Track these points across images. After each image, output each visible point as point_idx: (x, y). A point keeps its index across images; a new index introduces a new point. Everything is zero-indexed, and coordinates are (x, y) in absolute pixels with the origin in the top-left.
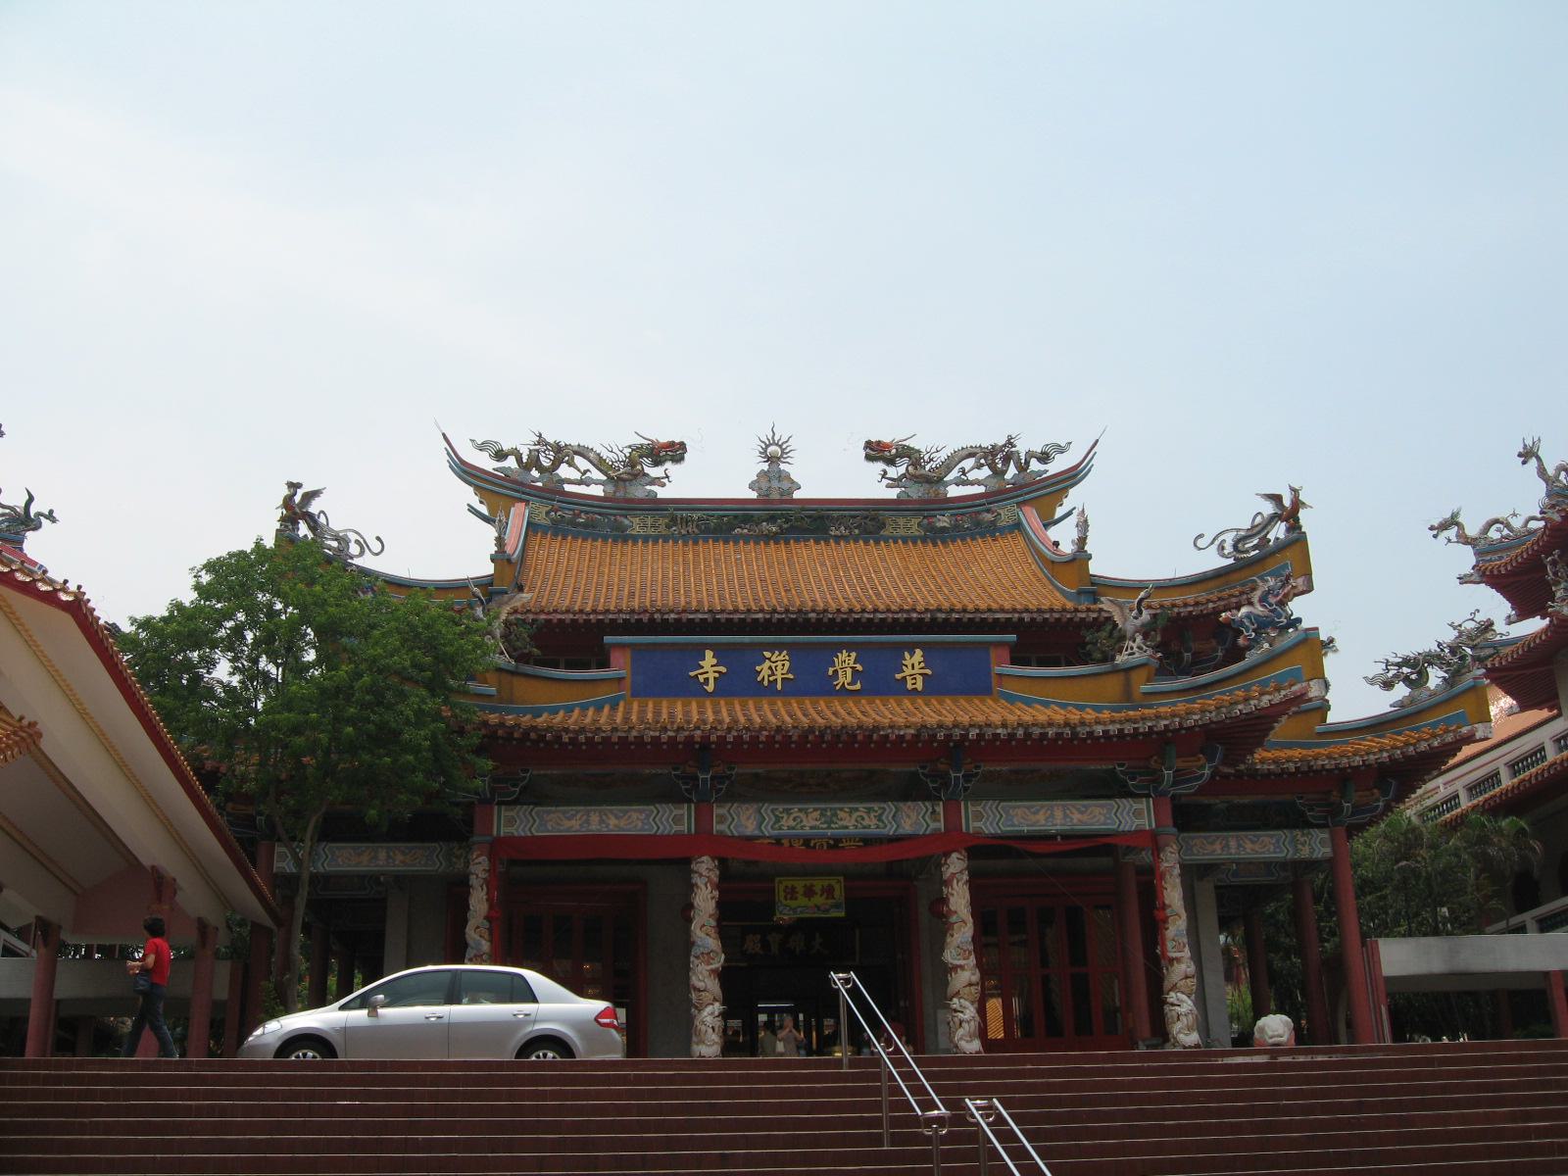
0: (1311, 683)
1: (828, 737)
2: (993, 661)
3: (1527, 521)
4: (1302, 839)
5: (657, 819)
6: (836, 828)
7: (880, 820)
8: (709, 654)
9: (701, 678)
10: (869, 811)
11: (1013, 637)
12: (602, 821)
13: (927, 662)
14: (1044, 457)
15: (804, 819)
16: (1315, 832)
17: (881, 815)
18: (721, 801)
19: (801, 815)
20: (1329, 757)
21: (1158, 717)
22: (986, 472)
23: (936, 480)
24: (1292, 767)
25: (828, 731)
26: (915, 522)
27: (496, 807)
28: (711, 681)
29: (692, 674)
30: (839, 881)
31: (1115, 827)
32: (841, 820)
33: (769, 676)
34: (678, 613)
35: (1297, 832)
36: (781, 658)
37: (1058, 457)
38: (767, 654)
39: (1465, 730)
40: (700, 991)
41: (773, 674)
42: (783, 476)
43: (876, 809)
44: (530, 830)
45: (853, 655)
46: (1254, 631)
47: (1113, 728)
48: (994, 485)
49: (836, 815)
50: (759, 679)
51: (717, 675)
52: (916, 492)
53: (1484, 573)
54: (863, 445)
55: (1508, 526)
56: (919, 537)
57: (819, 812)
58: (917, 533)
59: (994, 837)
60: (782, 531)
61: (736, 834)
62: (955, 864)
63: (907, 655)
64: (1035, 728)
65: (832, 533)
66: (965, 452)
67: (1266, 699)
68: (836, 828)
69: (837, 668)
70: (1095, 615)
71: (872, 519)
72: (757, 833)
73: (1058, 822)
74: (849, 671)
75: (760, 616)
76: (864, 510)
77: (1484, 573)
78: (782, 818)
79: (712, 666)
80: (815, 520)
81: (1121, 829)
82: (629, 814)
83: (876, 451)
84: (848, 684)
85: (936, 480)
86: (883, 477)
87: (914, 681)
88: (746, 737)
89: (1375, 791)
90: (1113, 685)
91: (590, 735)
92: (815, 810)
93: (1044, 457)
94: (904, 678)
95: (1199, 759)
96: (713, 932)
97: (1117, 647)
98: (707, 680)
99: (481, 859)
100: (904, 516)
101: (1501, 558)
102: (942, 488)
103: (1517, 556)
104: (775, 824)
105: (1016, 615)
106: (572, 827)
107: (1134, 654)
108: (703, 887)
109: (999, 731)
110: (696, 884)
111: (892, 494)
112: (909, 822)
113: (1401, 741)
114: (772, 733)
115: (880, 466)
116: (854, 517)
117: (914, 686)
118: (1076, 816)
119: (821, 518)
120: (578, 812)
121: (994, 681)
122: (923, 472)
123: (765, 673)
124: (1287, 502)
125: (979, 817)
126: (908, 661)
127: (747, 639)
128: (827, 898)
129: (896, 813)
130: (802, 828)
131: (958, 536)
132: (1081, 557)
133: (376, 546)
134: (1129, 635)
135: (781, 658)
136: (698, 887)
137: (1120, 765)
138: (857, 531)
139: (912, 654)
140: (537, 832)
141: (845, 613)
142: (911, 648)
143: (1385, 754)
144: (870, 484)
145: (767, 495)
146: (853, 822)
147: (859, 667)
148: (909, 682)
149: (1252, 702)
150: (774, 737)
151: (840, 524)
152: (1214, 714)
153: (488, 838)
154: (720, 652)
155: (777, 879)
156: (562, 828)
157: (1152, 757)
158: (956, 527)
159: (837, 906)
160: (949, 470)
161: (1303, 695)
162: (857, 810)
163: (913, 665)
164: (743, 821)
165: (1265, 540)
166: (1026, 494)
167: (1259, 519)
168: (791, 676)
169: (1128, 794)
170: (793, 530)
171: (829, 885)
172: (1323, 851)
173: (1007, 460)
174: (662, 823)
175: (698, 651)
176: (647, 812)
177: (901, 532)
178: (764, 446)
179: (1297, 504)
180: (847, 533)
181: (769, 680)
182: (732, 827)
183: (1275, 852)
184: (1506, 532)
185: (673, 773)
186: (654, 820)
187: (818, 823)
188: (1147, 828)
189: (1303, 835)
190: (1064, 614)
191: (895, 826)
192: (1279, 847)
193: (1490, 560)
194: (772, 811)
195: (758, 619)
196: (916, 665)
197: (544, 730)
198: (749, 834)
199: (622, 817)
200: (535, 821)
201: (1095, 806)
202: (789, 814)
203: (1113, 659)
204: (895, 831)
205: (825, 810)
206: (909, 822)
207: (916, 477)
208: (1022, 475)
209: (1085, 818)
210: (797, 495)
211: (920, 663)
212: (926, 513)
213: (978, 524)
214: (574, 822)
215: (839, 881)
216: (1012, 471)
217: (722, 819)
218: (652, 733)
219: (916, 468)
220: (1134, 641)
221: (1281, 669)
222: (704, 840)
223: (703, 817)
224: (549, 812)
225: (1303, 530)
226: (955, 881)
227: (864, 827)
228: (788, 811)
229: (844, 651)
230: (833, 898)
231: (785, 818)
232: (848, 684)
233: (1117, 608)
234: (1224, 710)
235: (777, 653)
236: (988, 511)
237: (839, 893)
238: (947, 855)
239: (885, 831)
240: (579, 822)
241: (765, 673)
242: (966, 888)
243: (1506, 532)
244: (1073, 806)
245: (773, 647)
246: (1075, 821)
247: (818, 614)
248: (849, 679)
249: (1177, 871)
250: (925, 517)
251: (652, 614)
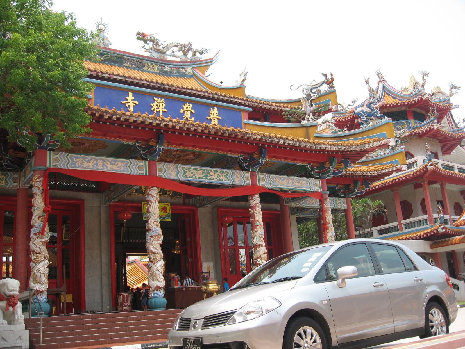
0: (390, 139)
1: (227, 134)
2: (242, 117)
3: (348, 106)
4: (338, 201)
5: (130, 167)
6: (209, 179)
7: (226, 177)
8: (130, 94)
9: (127, 105)
10: (222, 172)
11: (250, 109)
12: (104, 165)
13: (219, 114)
14: (201, 53)
15: (196, 174)
16: (342, 199)
17: (227, 175)
18: (161, 160)
19: (193, 171)
20: (360, 171)
21: (342, 145)
22: (181, 54)
23: (163, 53)
24: (351, 173)
25: (227, 132)
26: (156, 67)
27: (48, 152)
28: (132, 107)
29: (123, 102)
30: (168, 205)
31: (309, 189)
32: (211, 175)
33: (157, 109)
34: (109, 74)
35: (337, 198)
36: (161, 101)
37: (206, 53)
38: (156, 99)
39: (398, 166)
40: (154, 254)
41: (158, 108)
42: (105, 38)
43: (225, 172)
44: (67, 165)
45: (191, 105)
46: (365, 117)
47: (328, 147)
48: (184, 59)
49: (209, 173)
50: (152, 109)
51: (134, 105)
52: (156, 55)
53: (336, 120)
54: (137, 33)
55: (342, 107)
56: (158, 73)
57: (202, 171)
58: (157, 72)
59: (269, 189)
60: (105, 60)
61: (167, 178)
62: (256, 200)
63: (211, 109)
64: (303, 143)
65: (125, 65)
66: (174, 45)
67: (375, 143)
68: (209, 179)
69: (185, 110)
70: (269, 107)
71: (140, 63)
72: (176, 178)
73: (291, 185)
74: (189, 112)
75: (145, 82)
76: (138, 58)
77: (336, 120)
78: (187, 172)
79: (132, 100)
80: (118, 58)
81: (311, 190)
82: (117, 163)
83: (142, 37)
84: (189, 118)
85: (163, 53)
86: (143, 47)
87: (214, 121)
88: (192, 129)
89: (364, 186)
90: (301, 131)
91: (118, 116)
92: (201, 170)
93: (201, 53)
94: (211, 119)
95: (342, 165)
96: (159, 224)
97: (302, 117)
98: (130, 106)
99: (41, 179)
100: (152, 64)
101: (341, 116)
102: (166, 56)
103: (351, 116)
104: (183, 174)
105: (243, 101)
106: (89, 166)
107: (309, 121)
108: (154, 202)
109: (290, 142)
110: (150, 201)
111: (147, 54)
112: (238, 179)
113: (380, 168)
114: (203, 129)
115: (142, 43)
116: (134, 60)
117: (214, 123)
118: (297, 184)
119: (121, 58)
120: (92, 159)
121: (243, 125)
122: (159, 48)
123: (155, 107)
124: (329, 76)
125: (263, 180)
126: (212, 112)
127: (148, 90)
128: (164, 213)
129: (233, 174)
130: (195, 177)
131: (172, 75)
132: (241, 88)
134: (307, 113)
135: (161, 101)
136: (151, 202)
137: (310, 165)
138: (134, 66)
139: (214, 109)
140: (70, 167)
141: (180, 88)
142: (213, 106)
144: (137, 48)
145: (99, 44)
147: (193, 111)
148: (212, 119)
149: (371, 144)
150: (204, 130)
151: (128, 62)
152: (359, 147)
153: (44, 168)
154: (135, 93)
155: (143, 203)
156: (84, 166)
157: (327, 162)
158: (171, 72)
159: (168, 216)
160: (168, 49)
161: (387, 143)
162: (217, 171)
163: (214, 114)
164: (170, 171)
165: (319, 91)
166: (196, 64)
167: (314, 83)
168: (165, 110)
169: (311, 176)
170: (109, 60)
171: (165, 207)
172: (345, 207)
173: (189, 50)
174: (133, 169)
175: (127, 91)
176: (126, 163)
177: (151, 70)
179: (332, 80)
180: (130, 66)
181: (157, 111)
182: (165, 174)
184: (342, 108)
185: (137, 144)
186: (129, 167)
187: (202, 176)
188: (320, 191)
189: (339, 200)
190: (259, 104)
191: (232, 180)
192: (332, 204)
193: (338, 116)
194: (182, 168)
195: (144, 84)
196: (215, 114)
197: (96, 110)
198: (173, 178)
199: (114, 164)
200: (69, 162)
201: (303, 180)
202: (190, 171)
203: (300, 122)
204: (233, 183)
205: (204, 170)
206: (238, 179)
207: (157, 50)
208: (194, 57)
209: (299, 185)
210: (110, 47)
211: (216, 113)
212: (160, 64)
213: (179, 72)
214: (89, 164)
215: (168, 205)
216: (190, 55)
217: (160, 170)
218: (149, 120)
219: (156, 46)
220: (309, 116)
221: (377, 133)
222: (152, 180)
223: (152, 168)
224: (77, 158)
225: (335, 88)
226: (257, 207)
227: (220, 180)
228: (189, 169)
229: (187, 103)
230: (166, 213)
231: (188, 172)
232: (189, 118)
233: (304, 102)
234: (362, 145)
235: (160, 99)
236: (182, 68)
237: (168, 210)
238: (253, 195)
239: (228, 183)
240: (92, 164)
241: (155, 107)
242: (261, 210)
243: (342, 108)
244: (296, 179)
245: (159, 96)
246: (296, 186)
247: (169, 86)
248: (189, 116)
249: (330, 210)
250: (160, 66)
251: (98, 73)
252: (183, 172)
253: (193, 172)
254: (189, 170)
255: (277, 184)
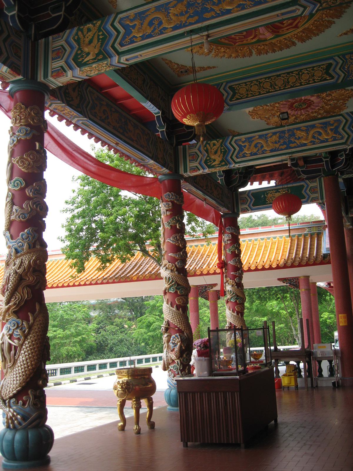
17: (337, 127)
32: (299, 138)
49: (293, 135)
104: (238, 153)
162: (313, 126)
187: (277, 146)
252: (237, 149)
253: (258, 143)
254: (249, 142)
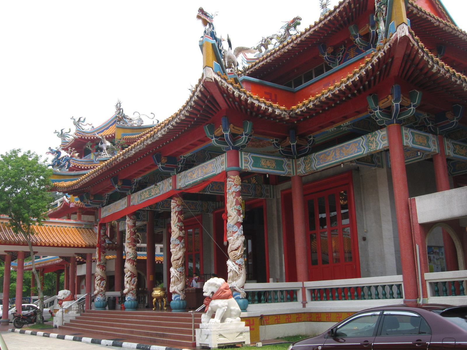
133: (152, 116)
143: (357, 75)
146: (154, 193)
178: (321, 2)
183: (358, 152)
255: (189, 180)
